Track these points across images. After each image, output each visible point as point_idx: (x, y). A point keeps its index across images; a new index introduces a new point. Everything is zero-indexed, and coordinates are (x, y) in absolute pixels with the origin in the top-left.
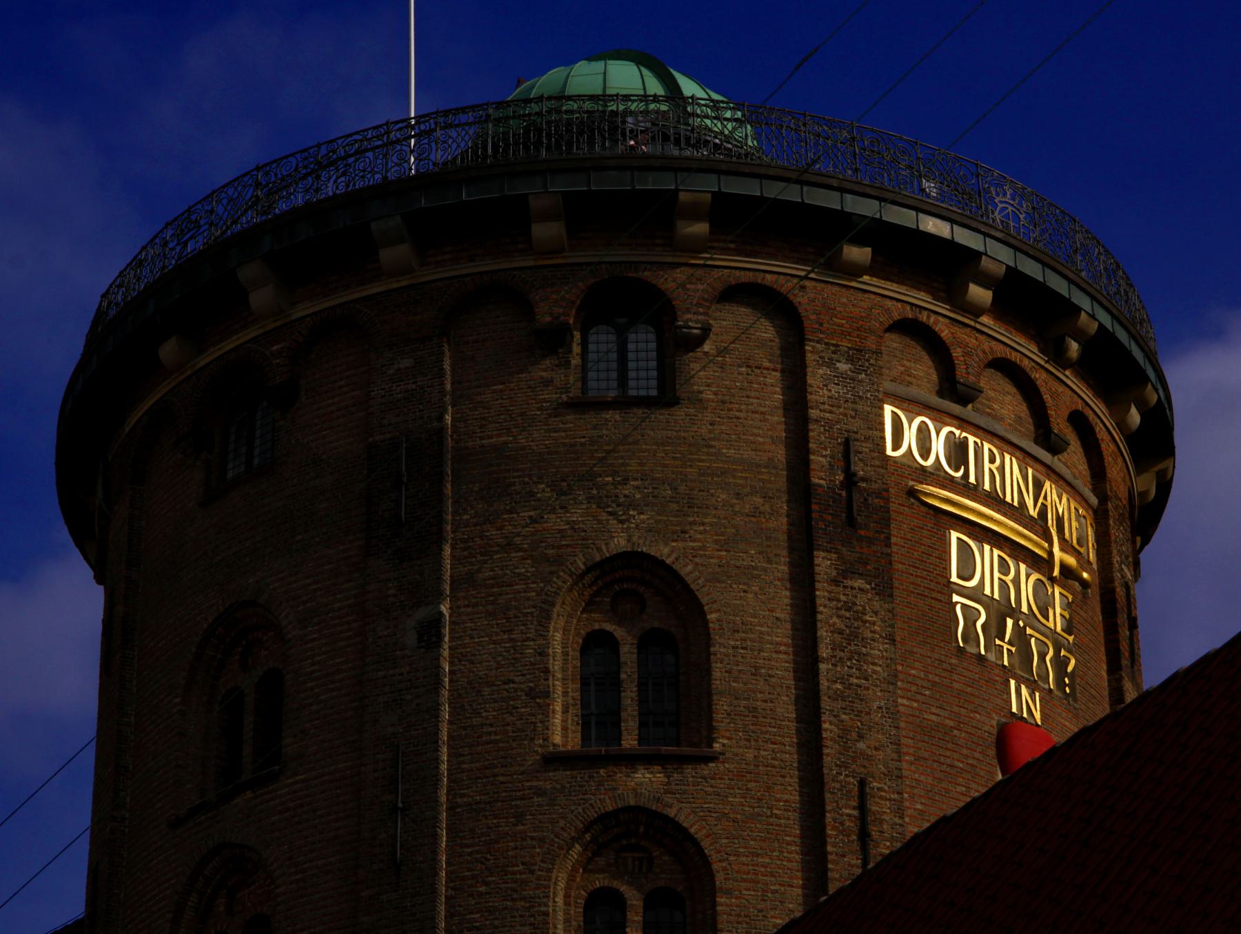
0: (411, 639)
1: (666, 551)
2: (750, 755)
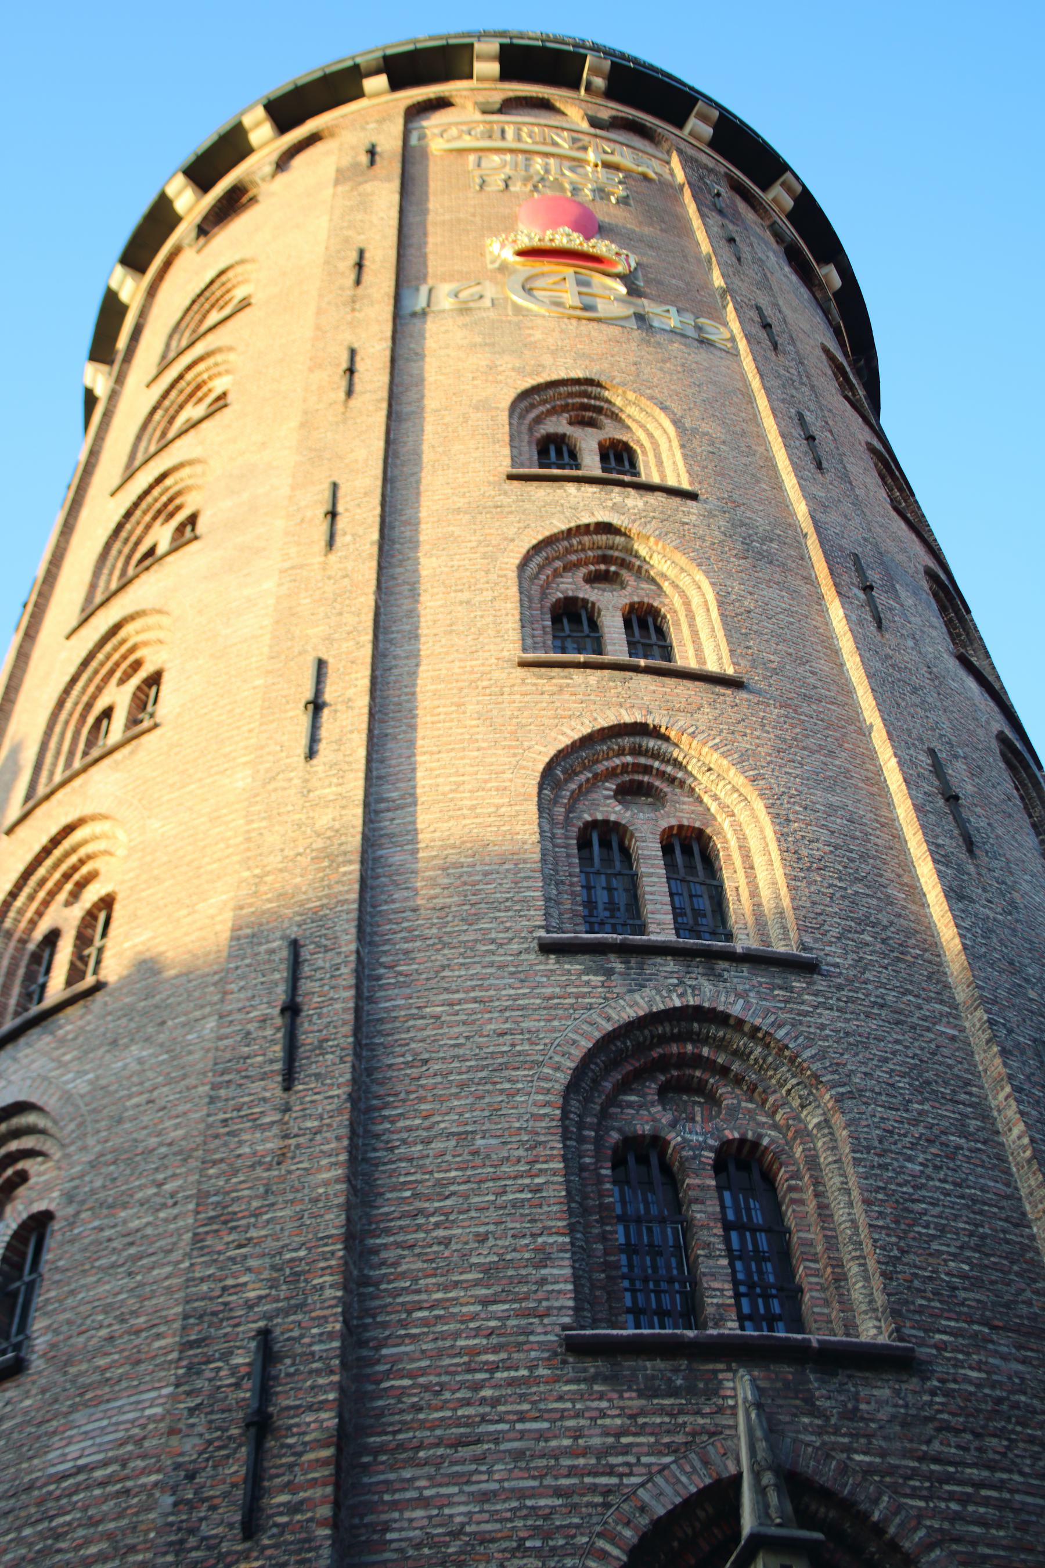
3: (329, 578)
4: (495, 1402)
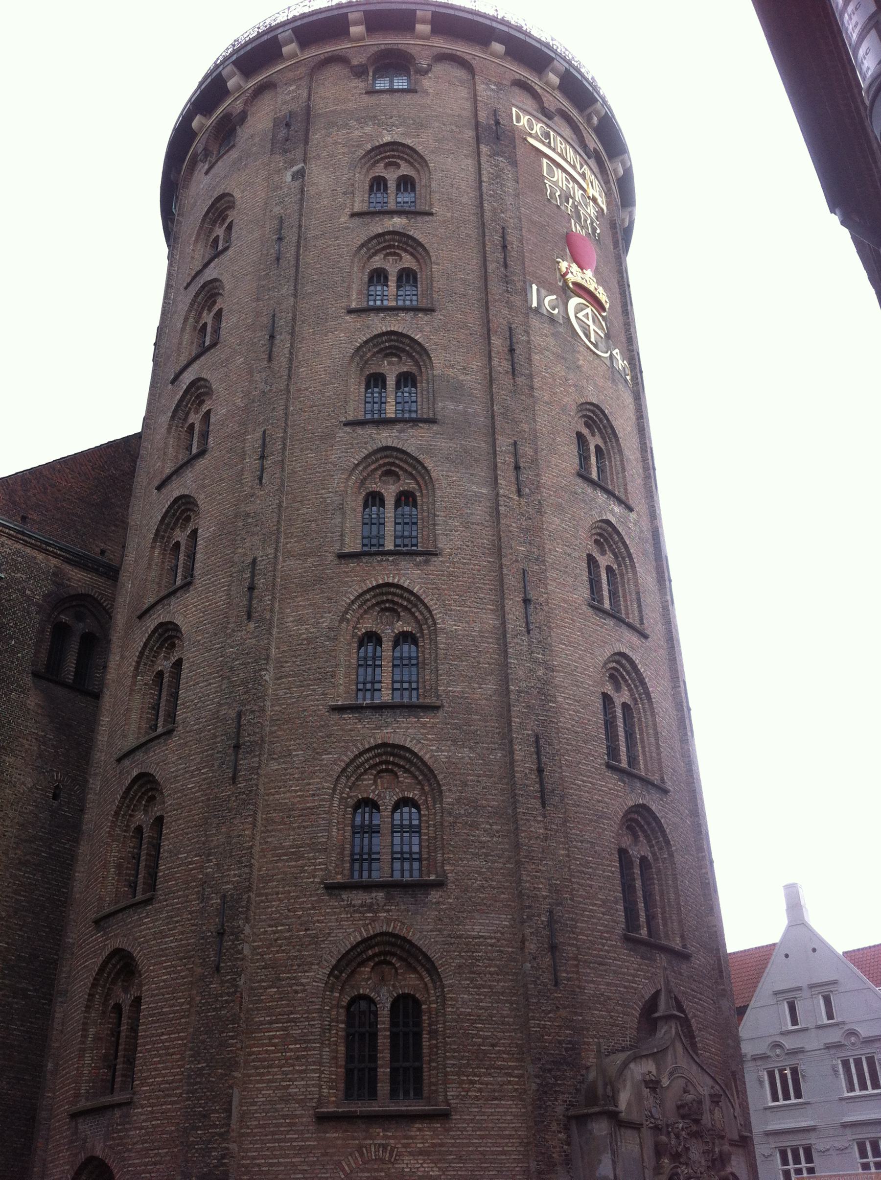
0: (289, 178)
1: (410, 141)
2: (449, 215)
3: (523, 515)
4: (608, 952)
